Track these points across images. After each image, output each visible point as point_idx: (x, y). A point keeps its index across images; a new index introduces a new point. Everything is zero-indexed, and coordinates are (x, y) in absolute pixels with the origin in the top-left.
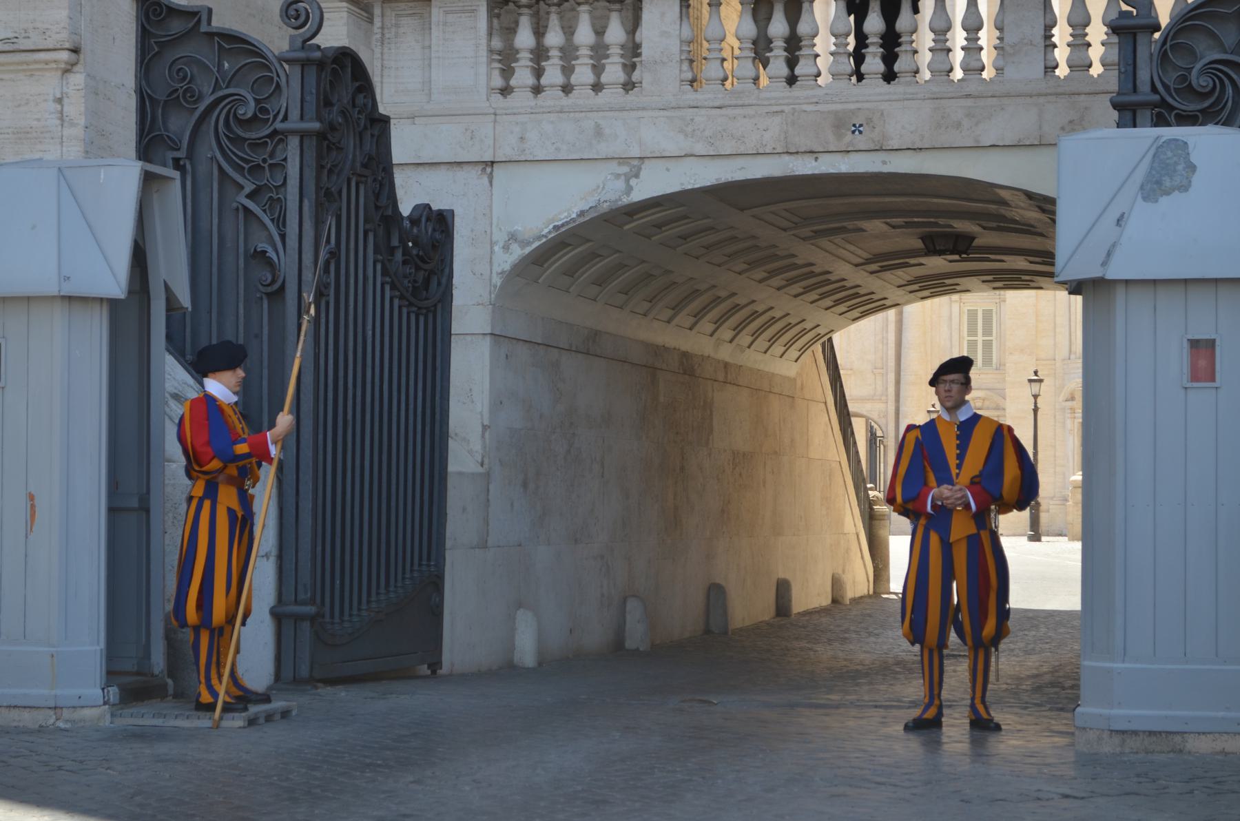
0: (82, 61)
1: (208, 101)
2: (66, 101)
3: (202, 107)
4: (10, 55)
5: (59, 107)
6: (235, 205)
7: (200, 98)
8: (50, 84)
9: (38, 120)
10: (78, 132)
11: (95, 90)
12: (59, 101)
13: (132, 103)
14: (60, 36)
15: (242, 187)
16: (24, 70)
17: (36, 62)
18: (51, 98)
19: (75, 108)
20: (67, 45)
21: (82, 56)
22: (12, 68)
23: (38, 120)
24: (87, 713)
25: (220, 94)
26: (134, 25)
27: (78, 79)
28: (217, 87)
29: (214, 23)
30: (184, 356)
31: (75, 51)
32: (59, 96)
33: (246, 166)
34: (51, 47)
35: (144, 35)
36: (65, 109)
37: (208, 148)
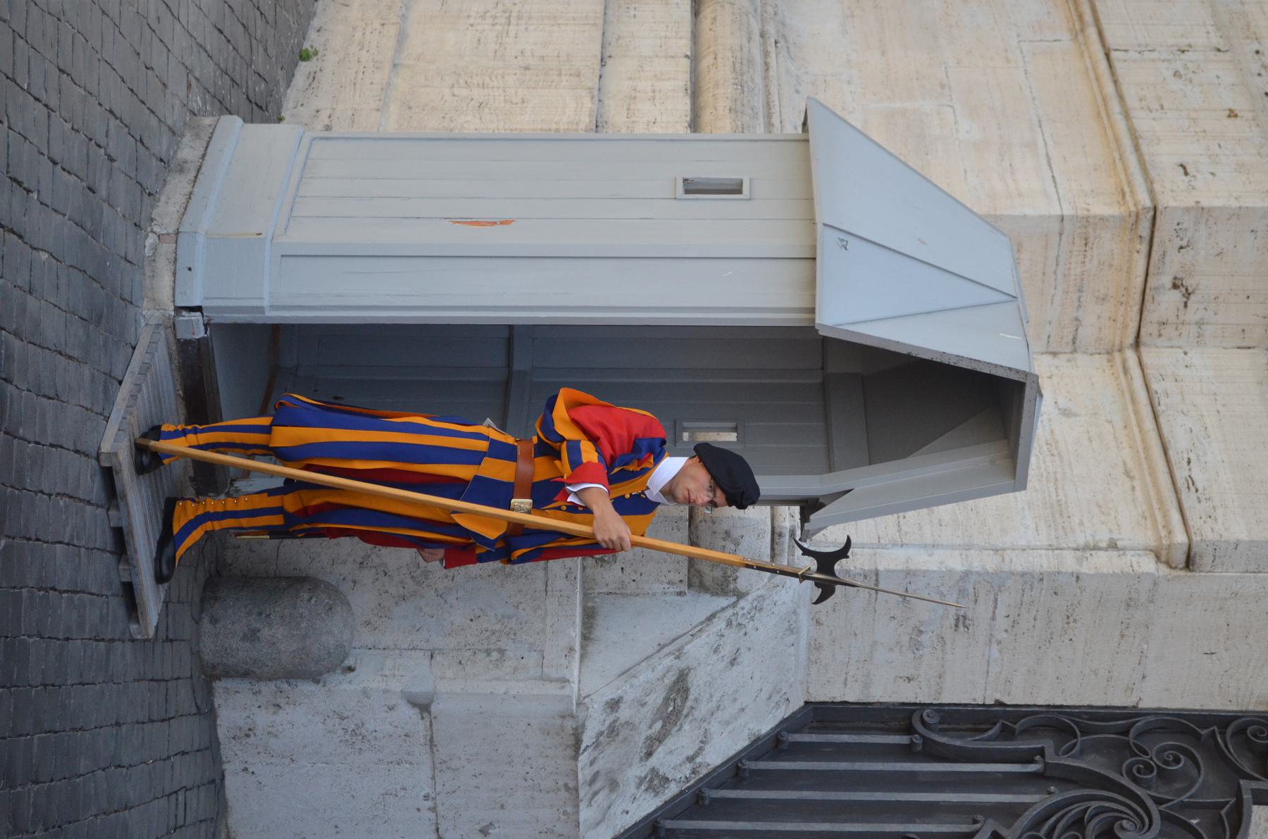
0: (1175, 573)
1: (1133, 787)
2: (1114, 554)
3: (1125, 781)
4: (1170, 486)
5: (1104, 545)
6: (980, 817)
7: (1135, 780)
8: (1135, 533)
9: (1081, 524)
10: (1069, 562)
11: (1132, 599)
12: (1113, 546)
13: (1118, 699)
14: (1205, 532)
15: (1009, 826)
16: (1151, 507)
17: (1165, 516)
18: (1116, 536)
19: (1103, 562)
20: (1196, 539)
21: (1183, 573)
22: (1152, 494)
23: (1081, 524)
24: (165, 281)
25: (1150, 803)
26: (1233, 707)
27: (1148, 565)
28: (1158, 801)
29: (1255, 808)
30: (750, 759)
31: (1189, 562)
32: (1120, 544)
33: (1042, 833)
34: (1191, 523)
35: (1222, 721)
36: (1101, 553)
37: (1058, 795)
